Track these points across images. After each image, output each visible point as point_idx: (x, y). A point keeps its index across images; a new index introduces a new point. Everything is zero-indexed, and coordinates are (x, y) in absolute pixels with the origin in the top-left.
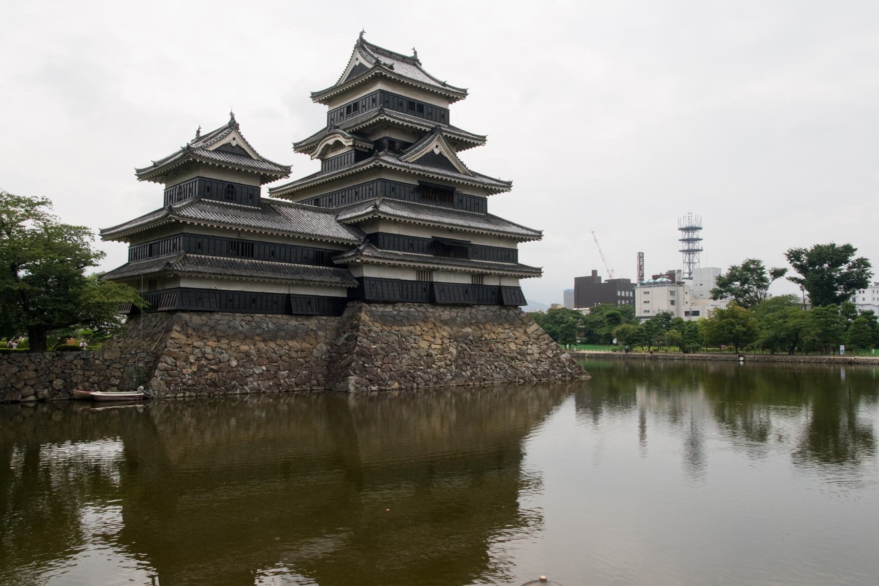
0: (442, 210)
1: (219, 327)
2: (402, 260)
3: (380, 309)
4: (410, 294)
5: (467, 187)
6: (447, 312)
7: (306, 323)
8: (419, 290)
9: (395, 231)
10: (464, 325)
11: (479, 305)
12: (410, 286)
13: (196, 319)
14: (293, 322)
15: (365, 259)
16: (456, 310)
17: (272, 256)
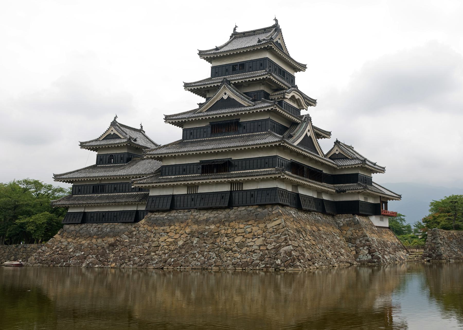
0: (228, 138)
1: (81, 232)
2: (159, 182)
3: (158, 215)
4: (182, 203)
5: (246, 115)
6: (206, 215)
7: (130, 227)
8: (189, 200)
9: (173, 163)
10: (213, 223)
11: (238, 206)
12: (182, 198)
13: (72, 227)
14: (122, 227)
15: (137, 185)
16: (215, 212)
17: (115, 190)
